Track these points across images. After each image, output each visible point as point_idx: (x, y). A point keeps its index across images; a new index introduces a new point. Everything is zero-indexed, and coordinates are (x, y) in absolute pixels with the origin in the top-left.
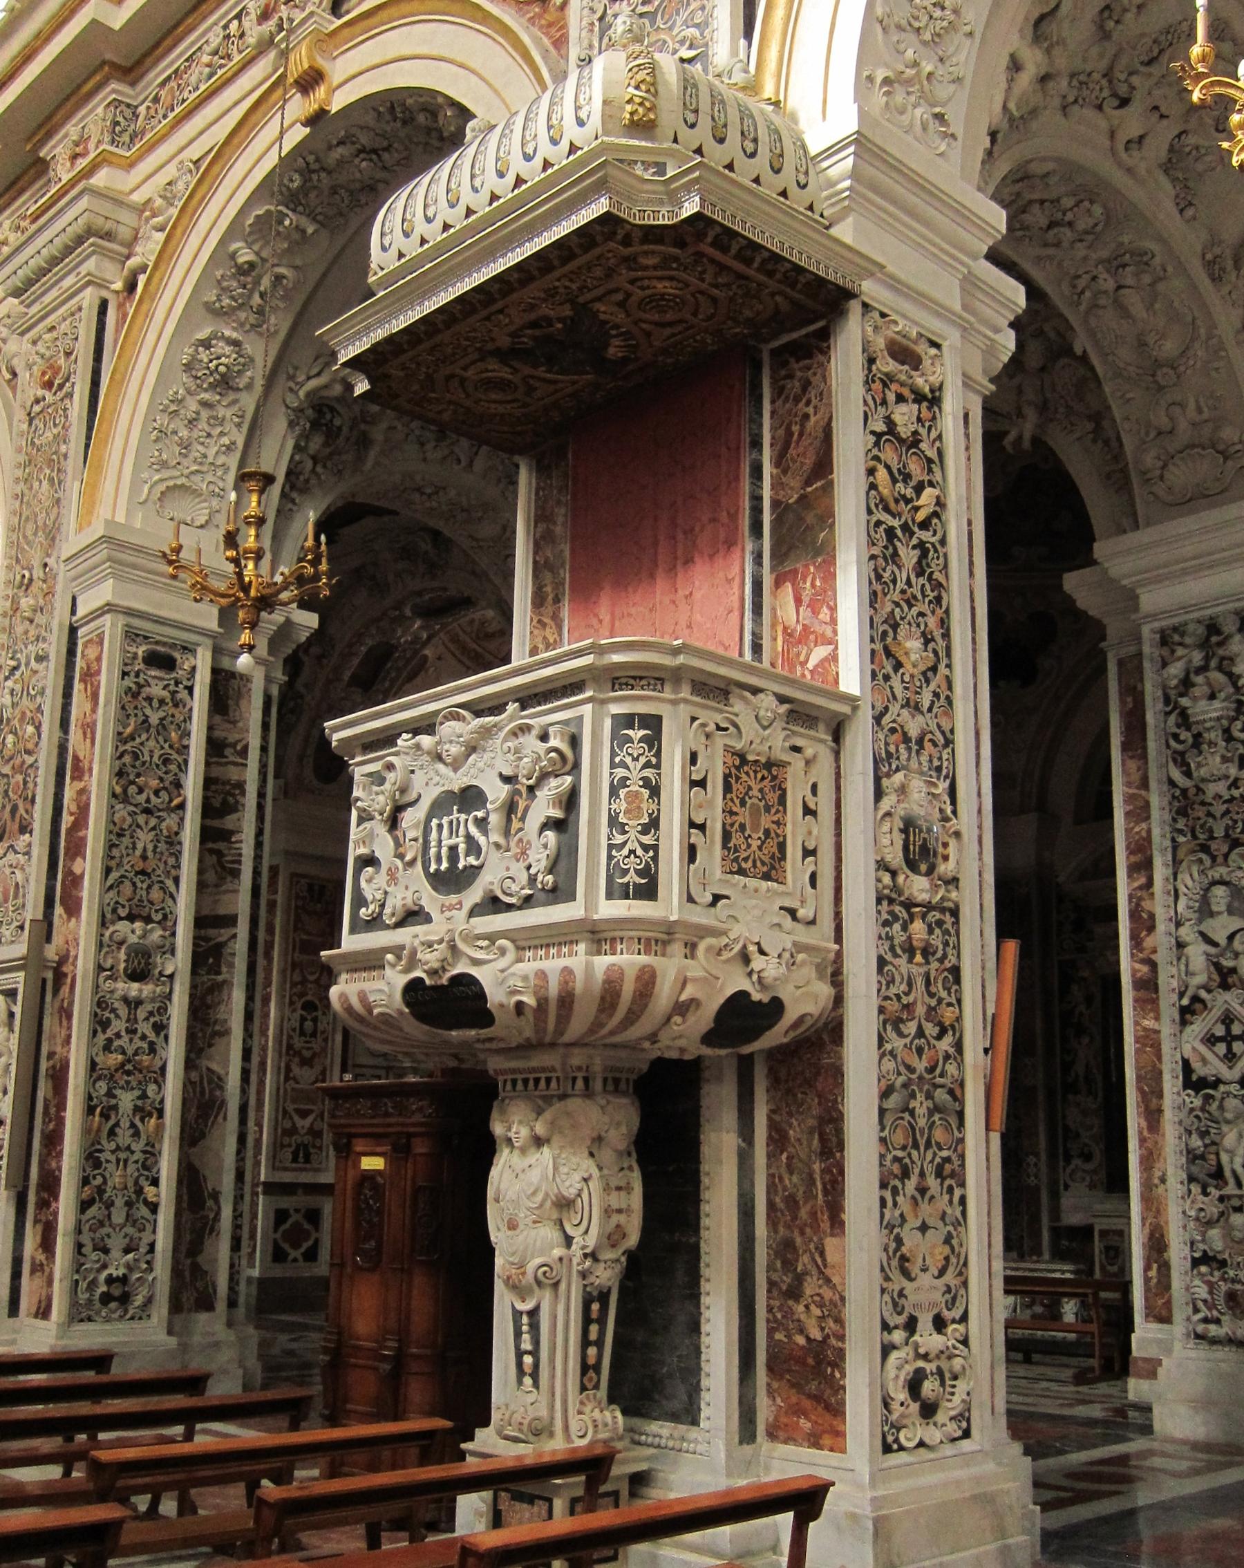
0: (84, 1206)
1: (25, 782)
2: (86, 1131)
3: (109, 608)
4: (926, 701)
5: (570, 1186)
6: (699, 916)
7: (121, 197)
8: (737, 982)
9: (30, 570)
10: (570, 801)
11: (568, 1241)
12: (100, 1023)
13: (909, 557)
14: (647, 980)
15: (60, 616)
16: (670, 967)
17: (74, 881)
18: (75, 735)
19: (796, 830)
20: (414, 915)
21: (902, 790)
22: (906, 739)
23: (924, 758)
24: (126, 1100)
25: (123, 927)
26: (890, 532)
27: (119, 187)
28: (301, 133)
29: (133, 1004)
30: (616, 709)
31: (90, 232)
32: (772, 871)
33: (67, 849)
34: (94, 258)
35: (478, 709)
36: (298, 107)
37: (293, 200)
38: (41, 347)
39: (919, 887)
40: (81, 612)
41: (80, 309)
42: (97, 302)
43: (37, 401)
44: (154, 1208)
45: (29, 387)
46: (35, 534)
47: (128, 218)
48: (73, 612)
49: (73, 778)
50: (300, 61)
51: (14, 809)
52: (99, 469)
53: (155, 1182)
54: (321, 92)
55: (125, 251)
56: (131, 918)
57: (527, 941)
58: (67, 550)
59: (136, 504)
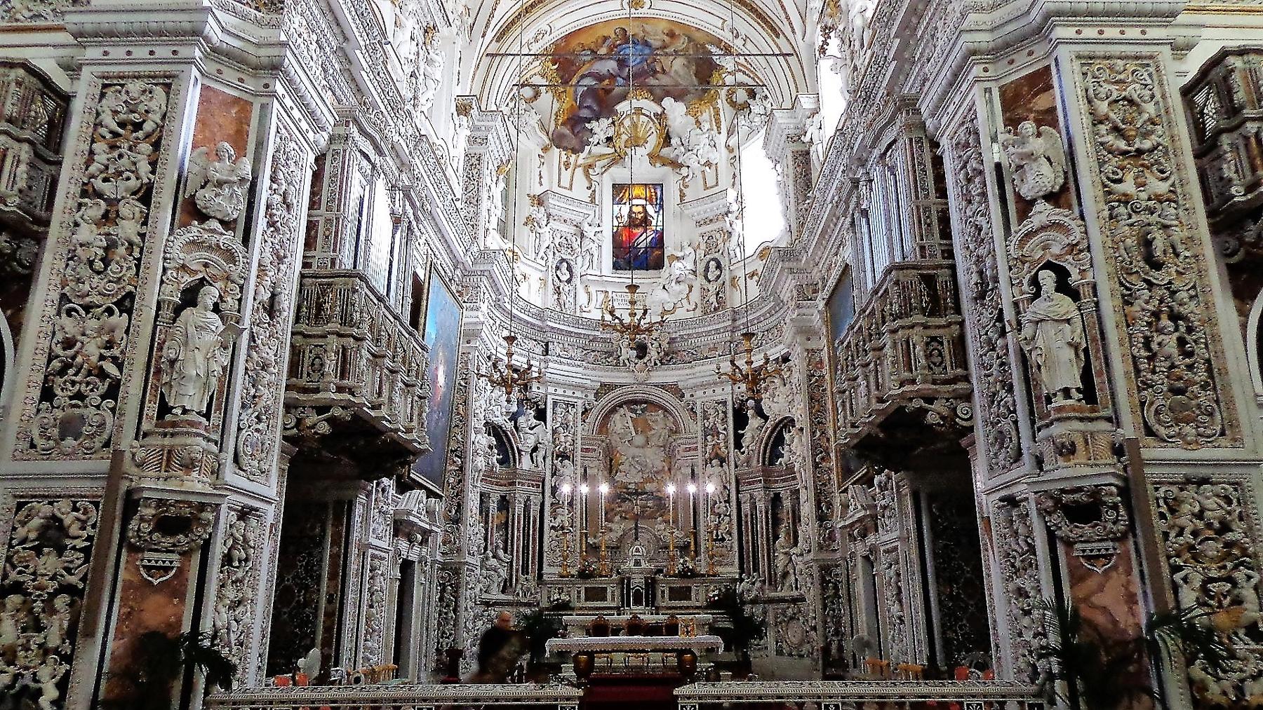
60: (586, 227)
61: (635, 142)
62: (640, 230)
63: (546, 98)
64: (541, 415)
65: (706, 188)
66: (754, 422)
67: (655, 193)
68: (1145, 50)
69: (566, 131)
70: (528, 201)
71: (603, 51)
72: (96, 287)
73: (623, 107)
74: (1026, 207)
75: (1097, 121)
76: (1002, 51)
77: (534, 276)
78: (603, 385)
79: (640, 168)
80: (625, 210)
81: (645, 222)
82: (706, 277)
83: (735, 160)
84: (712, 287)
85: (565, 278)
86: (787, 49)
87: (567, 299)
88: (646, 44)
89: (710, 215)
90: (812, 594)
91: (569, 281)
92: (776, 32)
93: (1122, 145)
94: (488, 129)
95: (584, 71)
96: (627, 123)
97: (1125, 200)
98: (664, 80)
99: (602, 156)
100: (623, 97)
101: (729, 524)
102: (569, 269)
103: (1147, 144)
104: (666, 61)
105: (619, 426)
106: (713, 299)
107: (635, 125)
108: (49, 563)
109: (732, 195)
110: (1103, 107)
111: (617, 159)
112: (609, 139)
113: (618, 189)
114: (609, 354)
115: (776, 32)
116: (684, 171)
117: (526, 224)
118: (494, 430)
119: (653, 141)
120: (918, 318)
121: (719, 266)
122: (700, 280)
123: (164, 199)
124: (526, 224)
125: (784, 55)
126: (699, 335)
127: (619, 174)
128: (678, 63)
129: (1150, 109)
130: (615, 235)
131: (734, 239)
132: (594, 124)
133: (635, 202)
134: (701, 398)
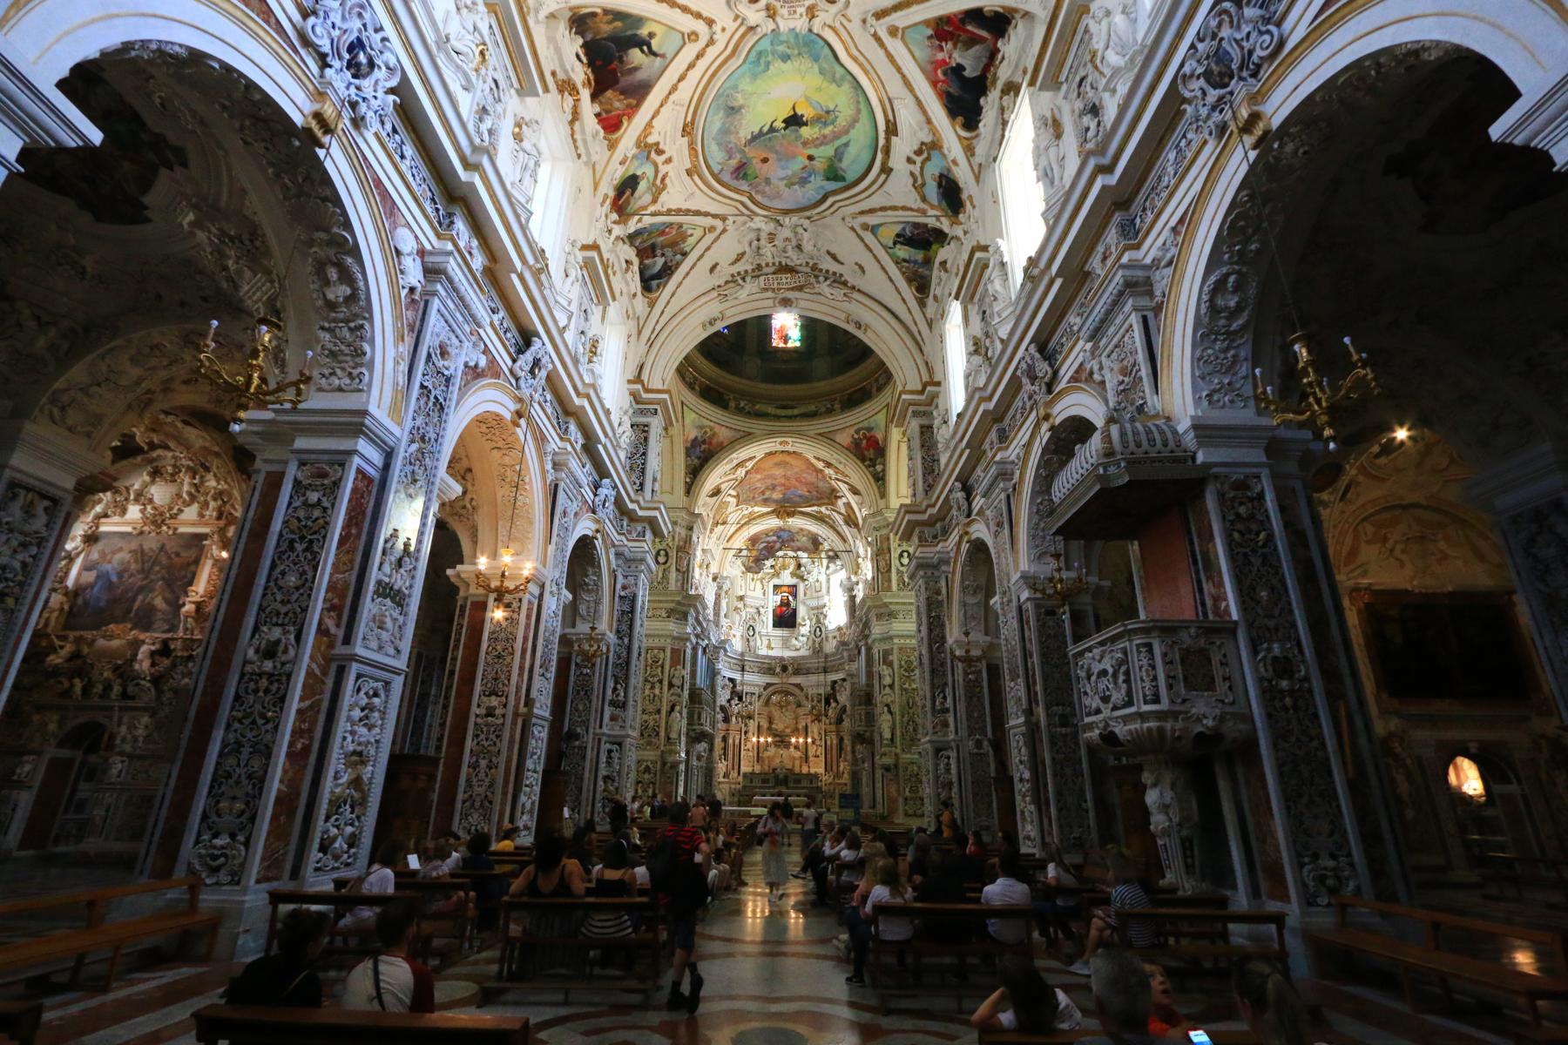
0: (1060, 810)
2: (1055, 784)
3: (1028, 599)
4: (1277, 613)
5: (1168, 800)
6: (1177, 708)
8: (1200, 729)
10: (1127, 673)
11: (1171, 820)
12: (1053, 743)
13: (1256, 561)
14: (1161, 730)
15: (1015, 603)
16: (1168, 726)
17: (1036, 694)
18: (1028, 645)
19: (1218, 672)
20: (1098, 711)
21: (1269, 649)
22: (1268, 629)
23: (1280, 634)
24: (1068, 771)
25: (1055, 708)
26: (1245, 555)
28: (1048, 434)
29: (1065, 736)
30: (1138, 642)
32: (1210, 685)
35: (1102, 644)
36: (1045, 426)
37: (1055, 452)
39: (1284, 684)
44: (1087, 811)
47: (1009, 467)
50: (1042, 413)
52: (1017, 553)
53: (1086, 801)
54: (1051, 420)
56: (1057, 705)
57: (1126, 719)
58: (1013, 581)
59: (1030, 562)
61: (784, 567)
63: (744, 553)
64: (740, 699)
66: (833, 705)
67: (793, 590)
72: (651, 708)
73: (780, 553)
75: (901, 666)
77: (738, 634)
81: (788, 604)
83: (828, 580)
87: (752, 643)
90: (848, 782)
92: (844, 540)
97: (906, 690)
100: (780, 549)
101: (821, 751)
108: (646, 776)
109: (826, 599)
111: (777, 575)
112: (772, 566)
113: (776, 587)
114: (770, 669)
115: (844, 540)
118: (723, 708)
119: (792, 567)
123: (666, 683)
134: (811, 692)
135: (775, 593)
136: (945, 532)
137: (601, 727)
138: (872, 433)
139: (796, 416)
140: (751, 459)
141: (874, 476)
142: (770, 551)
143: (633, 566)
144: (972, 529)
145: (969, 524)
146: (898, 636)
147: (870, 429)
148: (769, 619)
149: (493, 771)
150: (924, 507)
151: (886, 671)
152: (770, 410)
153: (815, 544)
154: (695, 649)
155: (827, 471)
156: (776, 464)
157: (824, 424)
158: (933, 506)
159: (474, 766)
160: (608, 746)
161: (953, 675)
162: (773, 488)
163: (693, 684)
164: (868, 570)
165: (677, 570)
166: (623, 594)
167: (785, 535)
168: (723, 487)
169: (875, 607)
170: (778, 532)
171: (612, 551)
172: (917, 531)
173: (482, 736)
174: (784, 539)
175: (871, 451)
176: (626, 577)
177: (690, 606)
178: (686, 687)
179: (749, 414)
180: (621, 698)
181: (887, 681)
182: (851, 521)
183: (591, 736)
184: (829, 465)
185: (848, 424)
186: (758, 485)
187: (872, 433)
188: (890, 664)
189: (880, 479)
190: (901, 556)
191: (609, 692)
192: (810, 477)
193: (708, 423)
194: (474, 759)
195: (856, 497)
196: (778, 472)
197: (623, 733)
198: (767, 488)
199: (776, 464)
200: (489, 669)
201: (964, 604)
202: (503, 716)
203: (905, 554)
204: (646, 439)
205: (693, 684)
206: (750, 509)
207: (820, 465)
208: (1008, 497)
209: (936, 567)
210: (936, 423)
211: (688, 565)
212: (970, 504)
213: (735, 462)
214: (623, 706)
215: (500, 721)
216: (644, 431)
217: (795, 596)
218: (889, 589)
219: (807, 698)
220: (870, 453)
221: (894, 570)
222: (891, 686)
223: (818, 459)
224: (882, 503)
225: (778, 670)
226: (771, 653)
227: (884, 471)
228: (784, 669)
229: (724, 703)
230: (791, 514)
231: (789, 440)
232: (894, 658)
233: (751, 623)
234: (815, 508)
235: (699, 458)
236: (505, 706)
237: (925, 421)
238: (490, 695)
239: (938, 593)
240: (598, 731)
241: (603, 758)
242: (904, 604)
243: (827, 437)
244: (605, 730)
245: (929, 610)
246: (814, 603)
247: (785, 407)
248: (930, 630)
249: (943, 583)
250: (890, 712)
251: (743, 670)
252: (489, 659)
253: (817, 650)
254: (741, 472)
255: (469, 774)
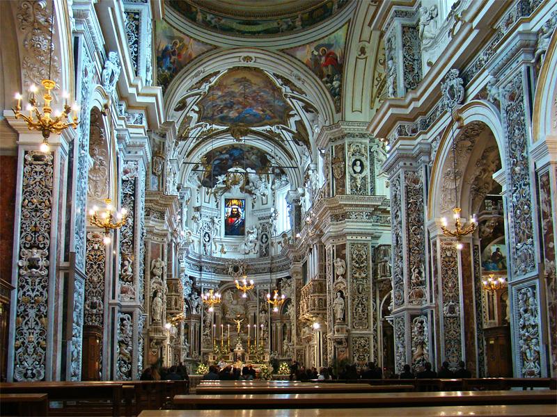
1: (526, 223)
7: (529, 32)
9: (516, 158)
27: (527, 29)
31: (522, 46)
33: (545, 241)
34: (523, 55)
38: (507, 88)
40: (538, 167)
41: (520, 72)
42: (526, 68)
43: (509, 106)
45: (504, 103)
46: (516, 147)
48: (535, 168)
49: (544, 219)
51: (524, 232)
52: (537, 121)
55: (533, 49)
60: (215, 219)
61: (235, 183)
62: (236, 219)
63: (201, 168)
65: (263, 204)
68: (366, 242)
69: (208, 180)
70: (193, 210)
71: (224, 152)
74: (338, 276)
75: (353, 259)
76: (336, 237)
77: (196, 240)
78: (221, 281)
79: (236, 192)
80: (230, 210)
81: (238, 215)
82: (262, 241)
84: (264, 246)
85: (207, 240)
86: (295, 166)
87: (207, 248)
88: (241, 150)
89: (264, 216)
91: (209, 241)
92: (291, 158)
93: (357, 265)
94: (185, 194)
95: (217, 158)
96: (232, 175)
97: (356, 278)
98: (248, 162)
99: (221, 188)
102: (209, 236)
103: (362, 265)
104: (249, 156)
105: (227, 297)
106: (264, 250)
107: (235, 176)
109: (272, 210)
110: (354, 256)
111: (227, 189)
114: (224, 270)
115: (291, 158)
116: (254, 196)
117: (192, 219)
120: (317, 294)
121: (267, 237)
122: (259, 243)
124: (192, 219)
125: (294, 168)
126: (259, 264)
127: (227, 195)
128: (253, 157)
129: (365, 257)
130: (226, 220)
131: (273, 228)
132: (219, 178)
133: (233, 207)
135: (226, 206)
136: (426, 126)
137: (114, 298)
138: (332, 50)
139: (259, 32)
140: (216, 74)
141: (330, 92)
142: (223, 169)
143: (133, 150)
144: (464, 115)
145: (461, 111)
146: (351, 234)
147: (329, 46)
148: (222, 227)
149: (44, 319)
150: (408, 100)
151: (339, 263)
152: (235, 25)
153: (262, 163)
154: (170, 245)
155: (286, 90)
156: (237, 81)
157: (284, 42)
158: (418, 99)
159: (20, 315)
160: (122, 316)
161: (430, 252)
162: (230, 106)
163: (169, 276)
164: (319, 179)
165: (153, 173)
166: (124, 178)
167: (236, 153)
168: (189, 100)
169: (331, 208)
170: (233, 147)
171: (115, 133)
172: (398, 124)
173: (28, 287)
174: (235, 156)
175: (330, 66)
176: (126, 162)
177: (166, 205)
178: (165, 277)
179: (215, 28)
180: (129, 273)
181: (340, 271)
182: (301, 137)
183: (107, 306)
184: (286, 82)
185: (306, 44)
186: (219, 102)
187: (332, 50)
188: (343, 257)
189: (337, 95)
190: (354, 164)
191: (119, 267)
192: (267, 95)
193: (177, 34)
194: (22, 308)
195: (309, 116)
196: (237, 89)
197: (134, 304)
198: (226, 106)
199: (237, 81)
200: (28, 222)
201: (444, 189)
202: (48, 268)
203: (358, 163)
204: (138, 28)
205: (169, 276)
206: (208, 127)
207: (278, 83)
208: (528, 69)
209: (415, 158)
210: (423, 18)
211: (163, 170)
212: (466, 90)
213: (202, 76)
214: (132, 280)
215: (44, 273)
216: (135, 19)
217: (244, 209)
218: (343, 192)
219: (255, 293)
220: (328, 70)
221: (348, 176)
222: (344, 276)
223: (277, 76)
224: (337, 117)
225: (230, 270)
226: (223, 256)
227: (340, 86)
228: (236, 269)
229: (186, 297)
230: (245, 133)
231: (252, 55)
232: (347, 252)
233: (207, 230)
234: (268, 128)
235: (169, 69)
236: (48, 258)
237: (407, 22)
238: (31, 247)
239: (416, 181)
240: (112, 301)
241: (118, 325)
242: (357, 206)
243: (288, 53)
244: (117, 301)
245: (408, 198)
246: (263, 214)
247: (248, 23)
248: (408, 215)
249: (422, 173)
250: (342, 296)
251: (201, 270)
252: (26, 213)
253: (264, 253)
254: (205, 87)
255: (18, 323)
